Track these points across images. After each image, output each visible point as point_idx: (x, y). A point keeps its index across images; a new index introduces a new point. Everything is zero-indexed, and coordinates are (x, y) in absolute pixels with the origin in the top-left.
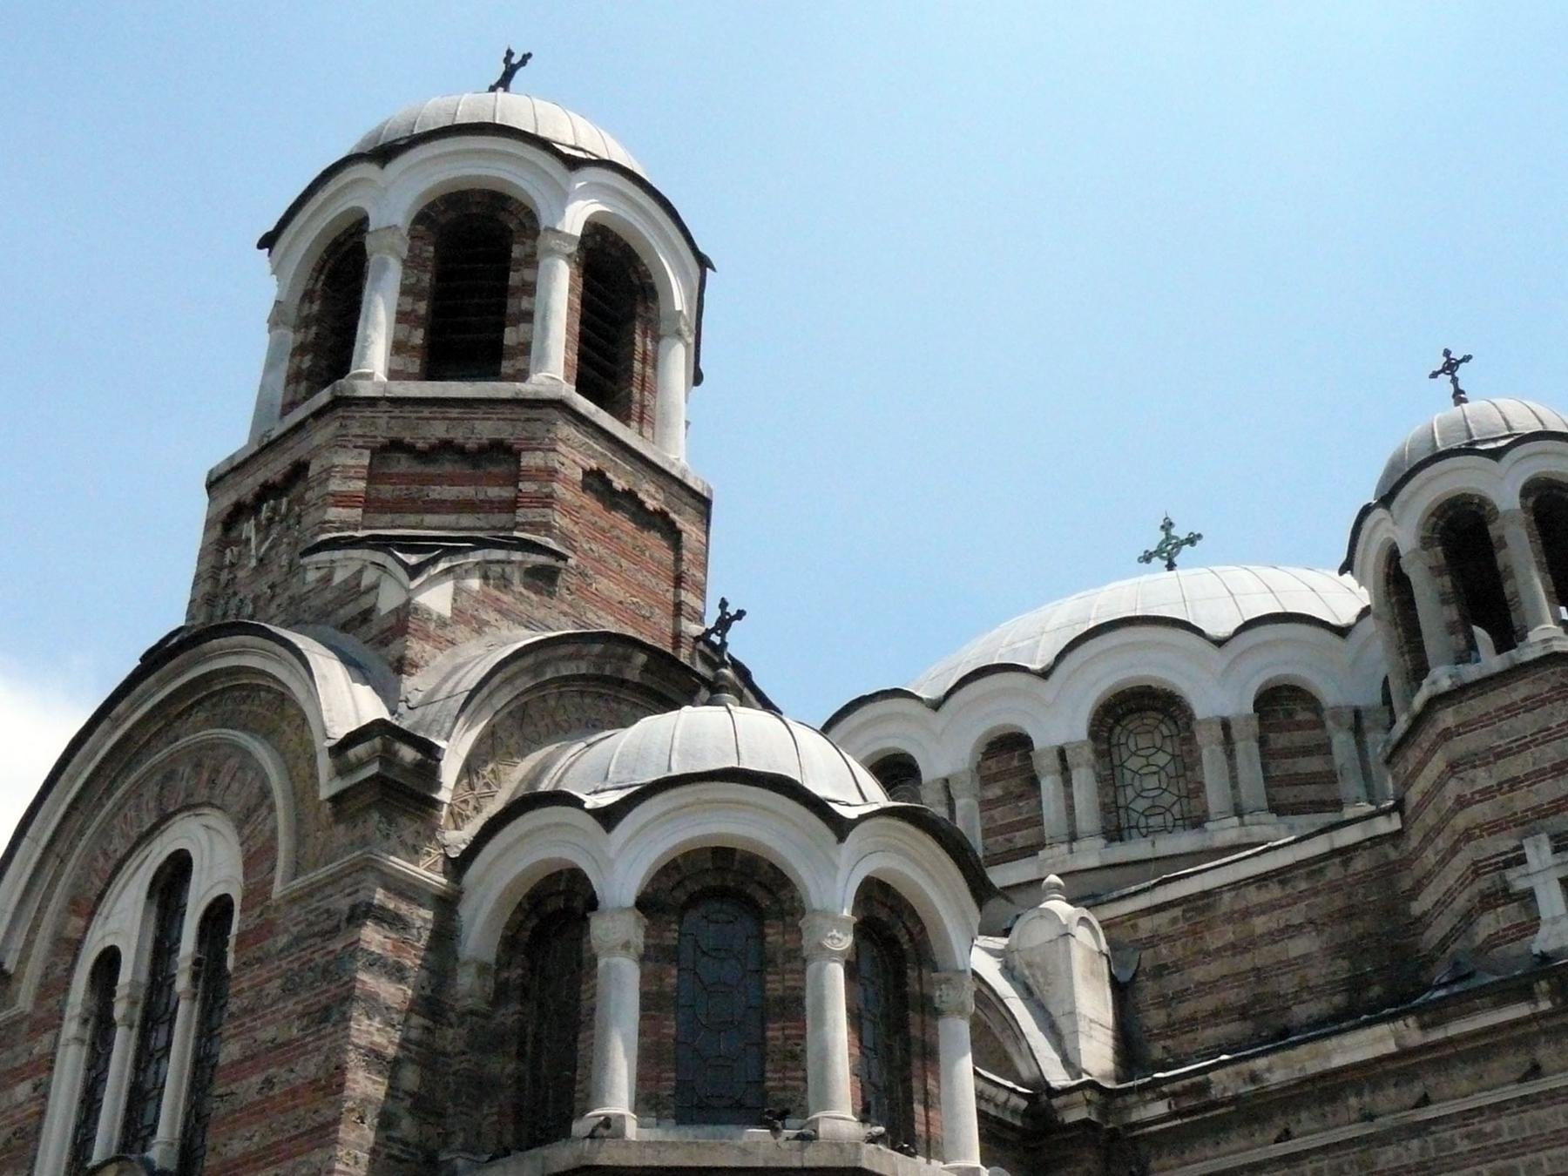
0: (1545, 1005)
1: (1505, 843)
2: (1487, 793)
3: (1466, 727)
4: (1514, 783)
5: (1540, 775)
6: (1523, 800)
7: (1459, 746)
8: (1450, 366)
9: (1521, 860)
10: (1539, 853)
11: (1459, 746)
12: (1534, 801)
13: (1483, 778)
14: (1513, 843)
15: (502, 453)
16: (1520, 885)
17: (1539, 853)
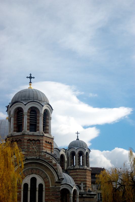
0: (81, 196)
1: (80, 182)
2: (79, 178)
3: (79, 172)
4: (81, 178)
5: (83, 178)
6: (82, 180)
7: (78, 173)
8: (78, 133)
9: (81, 184)
10: (82, 184)
11: (78, 173)
12: (82, 180)
13: (79, 177)
14: (80, 183)
15: (51, 143)
16: (81, 186)
17: (82, 184)
